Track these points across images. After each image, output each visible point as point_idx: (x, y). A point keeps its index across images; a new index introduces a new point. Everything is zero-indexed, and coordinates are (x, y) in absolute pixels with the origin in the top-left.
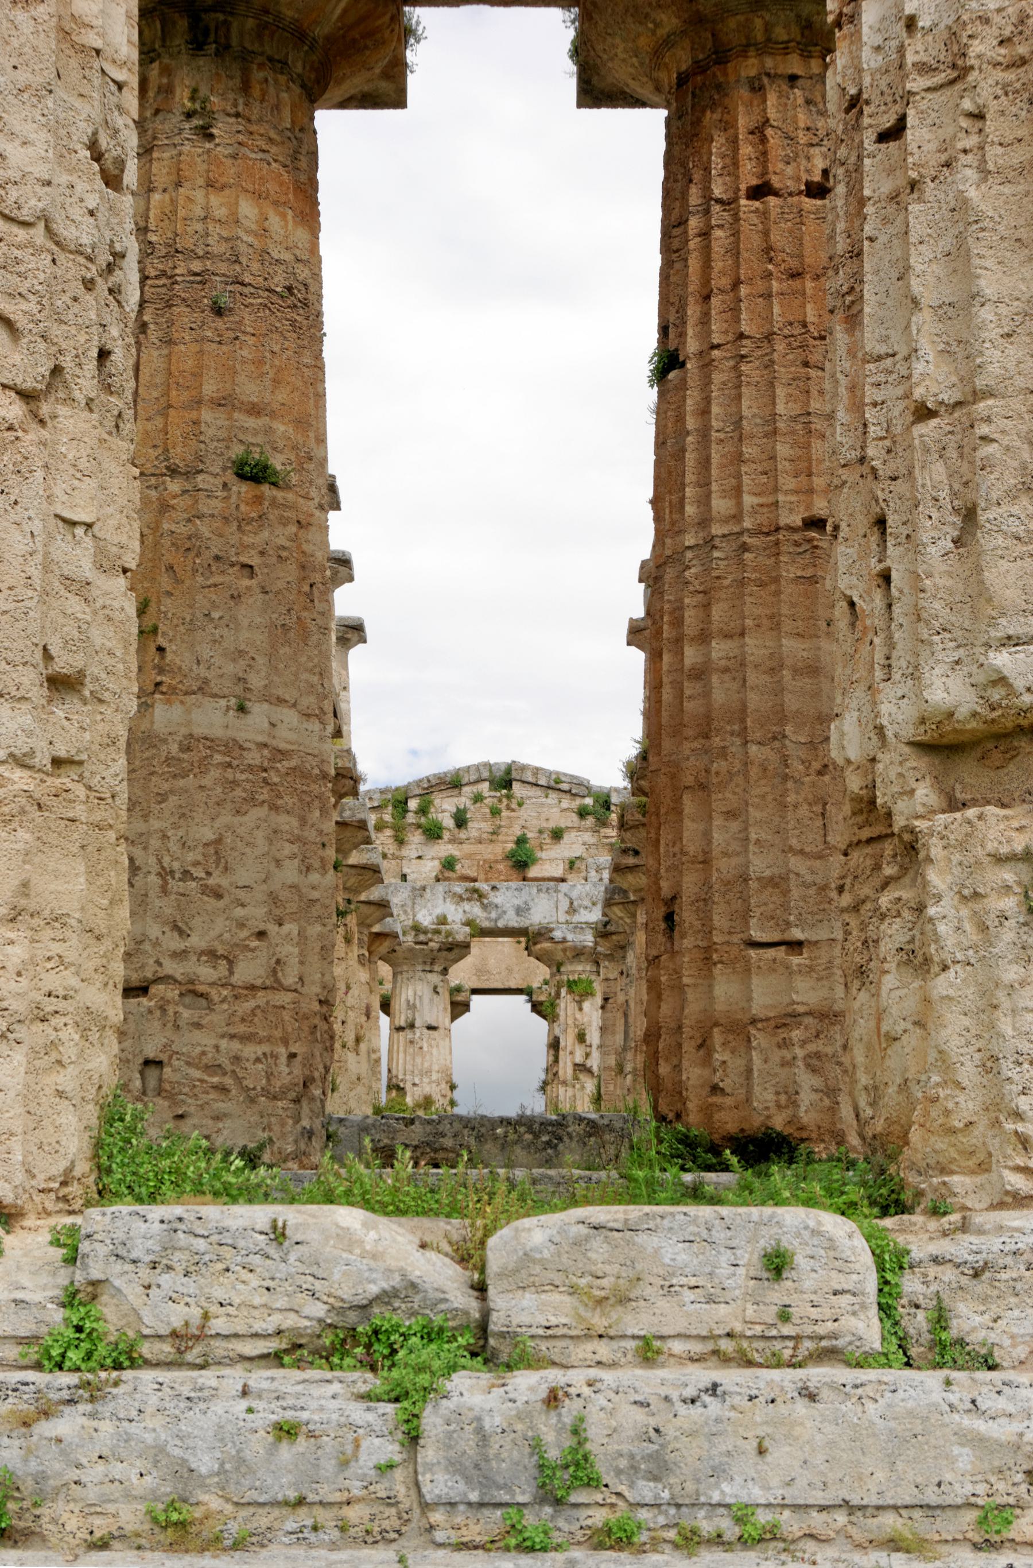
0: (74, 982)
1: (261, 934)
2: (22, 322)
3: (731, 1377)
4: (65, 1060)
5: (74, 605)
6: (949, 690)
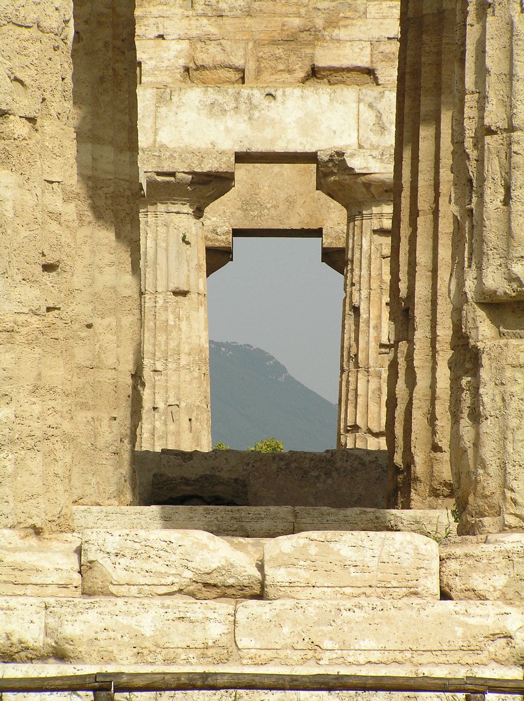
0: (59, 420)
1: (89, 326)
2: (27, 81)
3: (363, 601)
4: (57, 458)
5: (54, 226)
6: (494, 281)
